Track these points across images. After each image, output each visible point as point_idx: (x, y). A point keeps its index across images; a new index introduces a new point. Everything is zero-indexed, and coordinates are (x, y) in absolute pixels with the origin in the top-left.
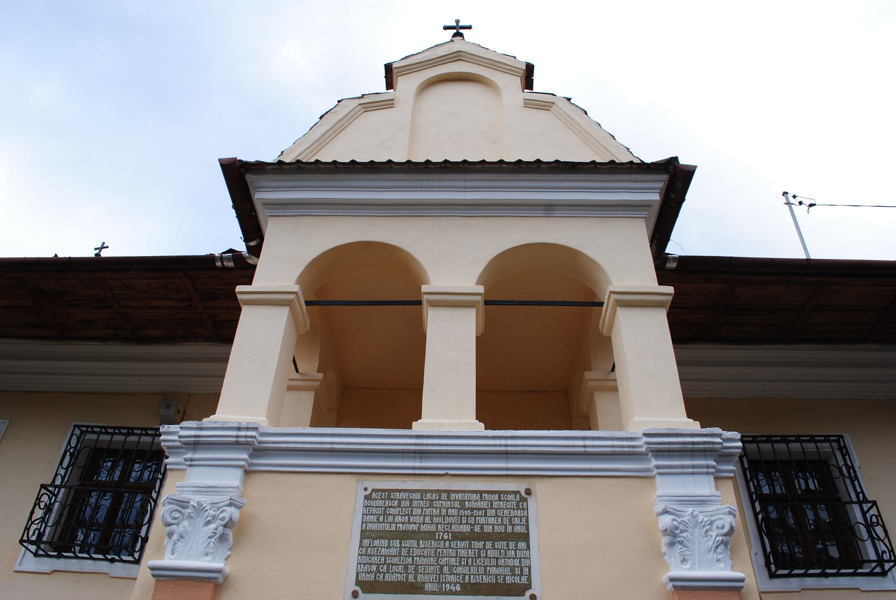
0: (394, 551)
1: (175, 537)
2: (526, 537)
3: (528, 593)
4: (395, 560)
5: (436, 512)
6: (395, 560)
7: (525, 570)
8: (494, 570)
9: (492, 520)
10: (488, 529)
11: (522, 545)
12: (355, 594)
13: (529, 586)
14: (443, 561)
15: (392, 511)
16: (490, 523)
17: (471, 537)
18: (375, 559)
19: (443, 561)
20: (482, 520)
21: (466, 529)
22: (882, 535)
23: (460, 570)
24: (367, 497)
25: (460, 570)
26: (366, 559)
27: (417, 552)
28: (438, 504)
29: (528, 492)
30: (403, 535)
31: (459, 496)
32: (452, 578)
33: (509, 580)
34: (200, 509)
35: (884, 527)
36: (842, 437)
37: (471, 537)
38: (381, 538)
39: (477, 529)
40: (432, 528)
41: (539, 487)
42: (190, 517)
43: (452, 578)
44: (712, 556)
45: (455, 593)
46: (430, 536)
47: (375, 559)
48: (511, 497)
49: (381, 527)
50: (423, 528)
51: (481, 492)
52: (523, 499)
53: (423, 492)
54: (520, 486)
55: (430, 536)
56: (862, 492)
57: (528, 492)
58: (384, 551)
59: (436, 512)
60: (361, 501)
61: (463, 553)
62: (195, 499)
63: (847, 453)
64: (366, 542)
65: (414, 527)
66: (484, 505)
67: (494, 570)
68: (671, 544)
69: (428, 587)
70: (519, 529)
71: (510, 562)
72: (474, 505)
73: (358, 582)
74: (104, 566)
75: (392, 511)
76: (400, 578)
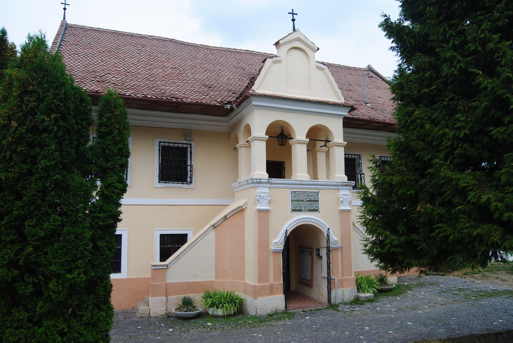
0: (297, 204)
1: (260, 203)
2: (318, 201)
3: (319, 211)
4: (297, 205)
5: (304, 196)
6: (297, 205)
7: (318, 207)
8: (313, 207)
9: (313, 198)
10: (312, 199)
11: (318, 202)
12: (292, 212)
13: (319, 210)
14: (305, 205)
15: (296, 196)
16: (313, 198)
17: (310, 201)
18: (294, 205)
19: (305, 205)
20: (311, 198)
21: (309, 199)
22: (364, 182)
23: (308, 207)
24: (292, 193)
25: (308, 207)
26: (293, 205)
27: (301, 204)
28: (304, 194)
29: (319, 192)
30: (299, 201)
31: (307, 193)
32: (307, 209)
33: (316, 209)
34: (263, 197)
35: (364, 180)
36: (361, 155)
37: (310, 201)
38: (294, 201)
39: (310, 199)
40: (303, 199)
41: (321, 191)
42: (262, 199)
43: (307, 209)
44: (347, 205)
45: (307, 211)
46: (303, 201)
47: (294, 205)
48: (316, 193)
49: (294, 199)
50: (302, 199)
51: (311, 192)
52: (318, 193)
53: (301, 192)
54: (317, 191)
55: (303, 201)
56: (362, 170)
57: (319, 192)
58: (295, 204)
59: (304, 196)
60: (290, 194)
61: (308, 204)
62: (263, 195)
63: (361, 159)
64: (292, 202)
65: (300, 199)
66: (311, 195)
67: (313, 207)
68: (341, 203)
69: (303, 210)
70: (317, 199)
71: (316, 206)
72: (310, 195)
73: (292, 210)
74: (180, 185)
75: (296, 196)
76: (299, 209)
